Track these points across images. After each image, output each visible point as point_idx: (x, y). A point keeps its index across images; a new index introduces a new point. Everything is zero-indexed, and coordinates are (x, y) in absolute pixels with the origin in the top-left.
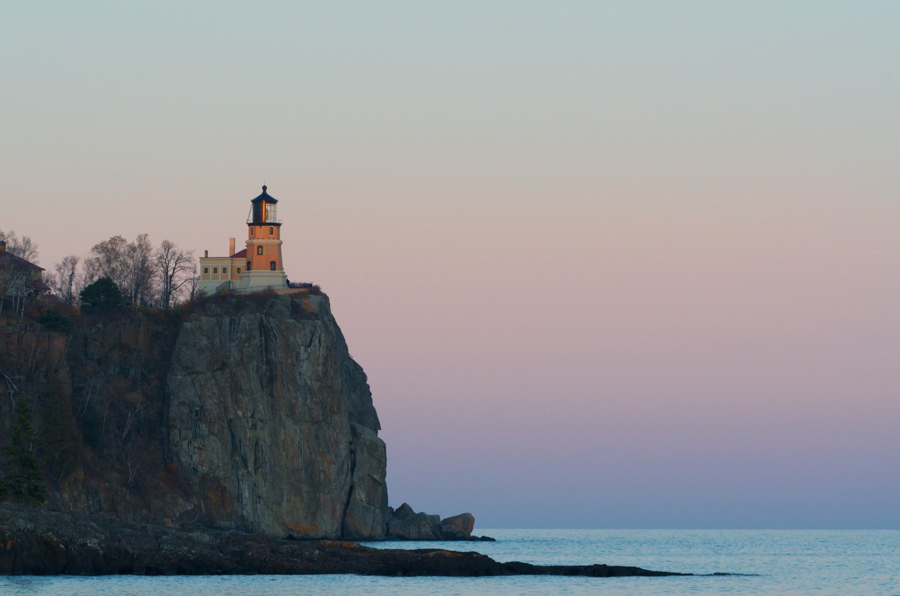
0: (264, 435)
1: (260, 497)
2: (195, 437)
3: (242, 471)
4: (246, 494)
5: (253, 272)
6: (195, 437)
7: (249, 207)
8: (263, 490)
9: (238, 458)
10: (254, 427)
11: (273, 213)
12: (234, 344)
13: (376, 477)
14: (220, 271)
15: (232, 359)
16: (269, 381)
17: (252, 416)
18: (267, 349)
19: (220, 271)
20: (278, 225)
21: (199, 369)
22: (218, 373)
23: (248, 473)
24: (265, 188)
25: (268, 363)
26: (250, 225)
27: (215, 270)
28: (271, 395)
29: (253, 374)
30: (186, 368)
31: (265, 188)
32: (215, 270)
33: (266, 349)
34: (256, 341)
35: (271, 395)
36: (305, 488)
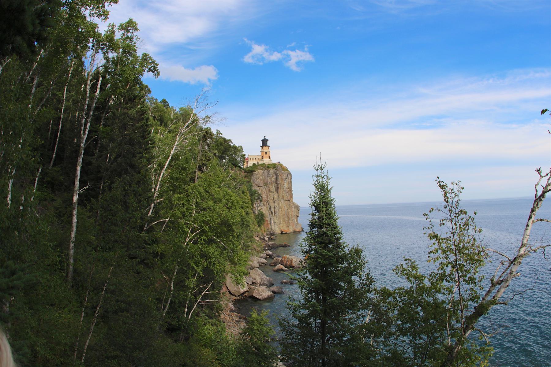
0: (276, 205)
1: (275, 223)
2: (260, 206)
3: (271, 215)
4: (272, 222)
5: (264, 159)
6: (260, 206)
7: (261, 142)
8: (276, 221)
9: (270, 212)
10: (274, 202)
11: (268, 143)
12: (269, 178)
13: (298, 215)
14: (254, 159)
15: (269, 182)
16: (277, 189)
17: (273, 199)
18: (277, 179)
19: (254, 159)
20: (269, 146)
21: (261, 185)
22: (265, 186)
23: (273, 216)
24: (265, 137)
25: (277, 184)
26: (261, 146)
27: (253, 159)
28: (278, 193)
29: (274, 187)
30: (257, 185)
31: (265, 137)
32: (253, 159)
33: (276, 179)
34: (274, 177)
35: (278, 193)
36: (286, 219)
